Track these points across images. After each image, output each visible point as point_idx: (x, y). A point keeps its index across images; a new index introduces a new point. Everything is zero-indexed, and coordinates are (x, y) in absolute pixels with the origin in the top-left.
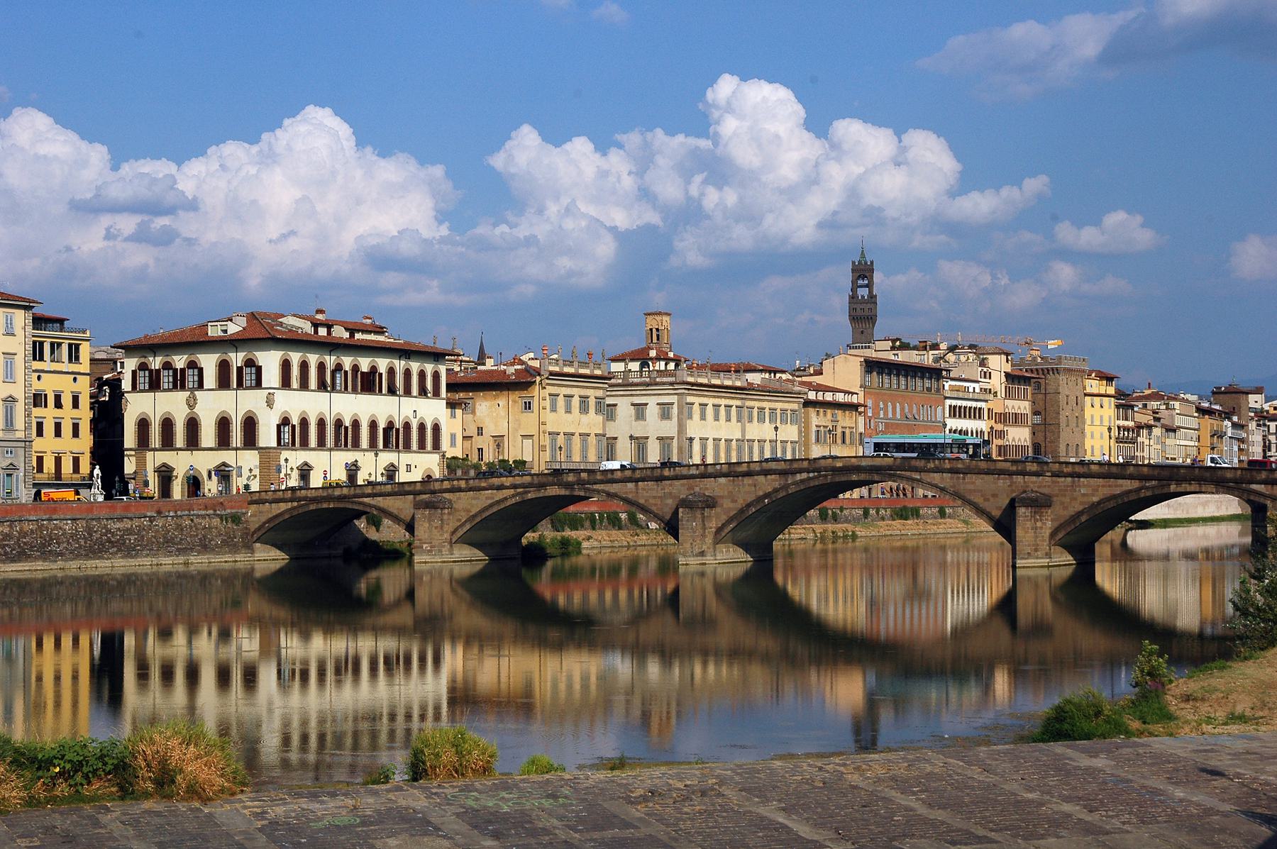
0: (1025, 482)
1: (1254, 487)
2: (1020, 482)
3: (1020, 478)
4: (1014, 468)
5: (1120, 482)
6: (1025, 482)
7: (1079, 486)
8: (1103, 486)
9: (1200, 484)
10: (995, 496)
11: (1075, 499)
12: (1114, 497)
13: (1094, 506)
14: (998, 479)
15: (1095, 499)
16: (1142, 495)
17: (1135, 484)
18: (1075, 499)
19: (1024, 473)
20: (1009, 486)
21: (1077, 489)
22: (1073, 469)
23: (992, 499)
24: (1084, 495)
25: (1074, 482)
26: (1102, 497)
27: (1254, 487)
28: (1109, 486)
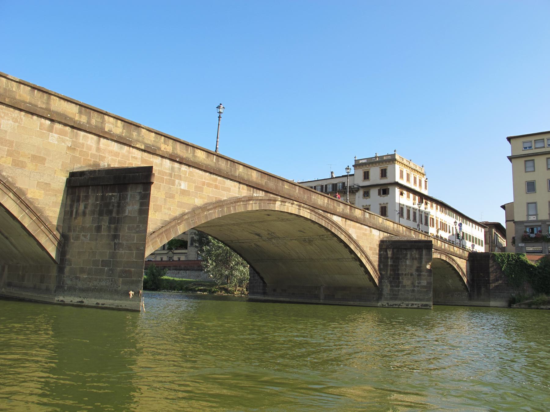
0: (98, 149)
1: (335, 218)
2: (90, 148)
3: (91, 139)
4: (83, 119)
5: (228, 183)
6: (98, 149)
7: (180, 178)
8: (209, 185)
9: (300, 206)
10: (38, 159)
11: (172, 197)
12: (219, 204)
13: (195, 211)
14: (51, 130)
15: (199, 202)
16: (249, 208)
17: (244, 191)
18: (172, 197)
19: (101, 134)
20: (69, 148)
21: (177, 181)
22: (174, 148)
23: (30, 166)
24: (184, 193)
25: (173, 169)
26: (206, 201)
27: (335, 218)
28: (216, 187)
